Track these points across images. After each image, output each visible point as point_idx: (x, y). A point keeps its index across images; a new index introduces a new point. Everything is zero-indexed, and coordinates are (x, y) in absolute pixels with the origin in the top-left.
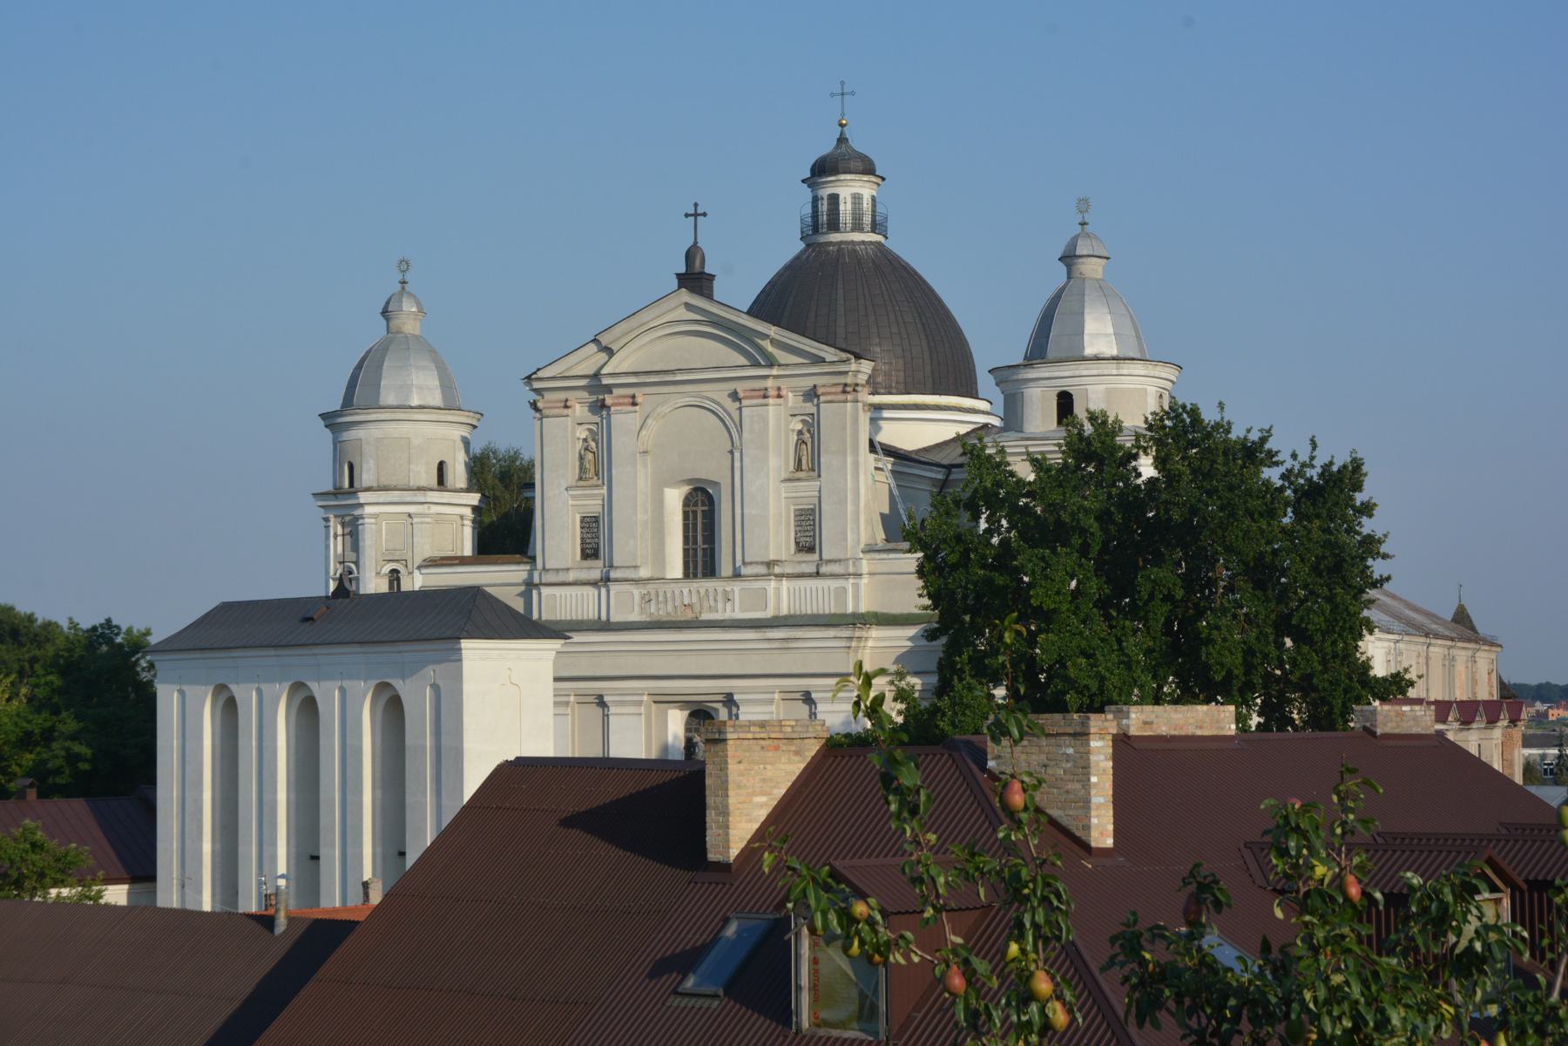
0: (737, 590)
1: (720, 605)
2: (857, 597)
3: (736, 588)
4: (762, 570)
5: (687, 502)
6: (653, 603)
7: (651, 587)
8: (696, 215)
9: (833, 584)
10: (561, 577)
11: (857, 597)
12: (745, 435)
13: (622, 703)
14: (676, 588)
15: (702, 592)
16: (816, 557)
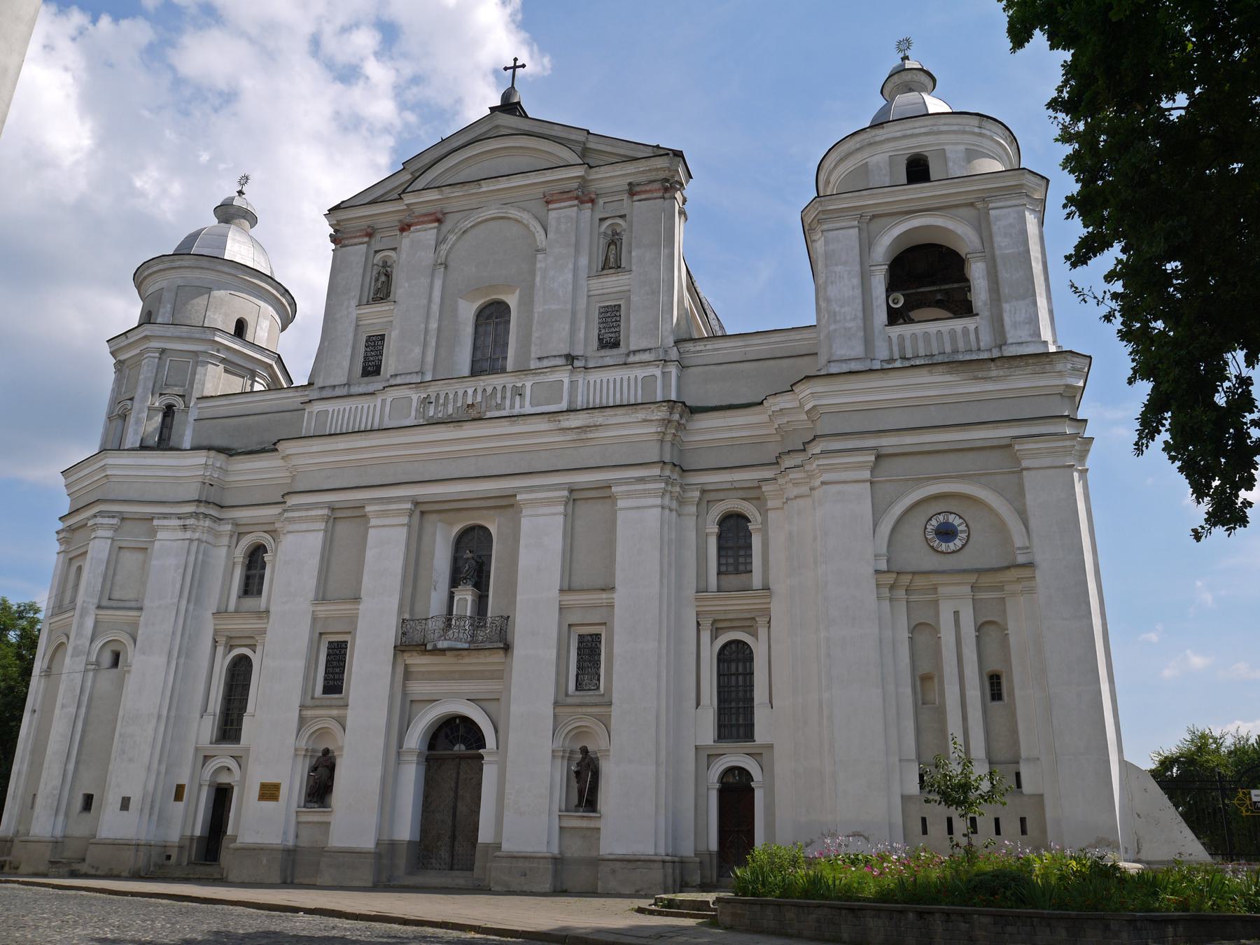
0: (528, 385)
1: (508, 402)
2: (666, 386)
4: (561, 361)
6: (432, 408)
7: (432, 390)
8: (515, 67)
9: (641, 373)
10: (338, 392)
11: (666, 386)
12: (551, 235)
13: (384, 514)
14: (460, 388)
15: (489, 390)
16: (623, 349)
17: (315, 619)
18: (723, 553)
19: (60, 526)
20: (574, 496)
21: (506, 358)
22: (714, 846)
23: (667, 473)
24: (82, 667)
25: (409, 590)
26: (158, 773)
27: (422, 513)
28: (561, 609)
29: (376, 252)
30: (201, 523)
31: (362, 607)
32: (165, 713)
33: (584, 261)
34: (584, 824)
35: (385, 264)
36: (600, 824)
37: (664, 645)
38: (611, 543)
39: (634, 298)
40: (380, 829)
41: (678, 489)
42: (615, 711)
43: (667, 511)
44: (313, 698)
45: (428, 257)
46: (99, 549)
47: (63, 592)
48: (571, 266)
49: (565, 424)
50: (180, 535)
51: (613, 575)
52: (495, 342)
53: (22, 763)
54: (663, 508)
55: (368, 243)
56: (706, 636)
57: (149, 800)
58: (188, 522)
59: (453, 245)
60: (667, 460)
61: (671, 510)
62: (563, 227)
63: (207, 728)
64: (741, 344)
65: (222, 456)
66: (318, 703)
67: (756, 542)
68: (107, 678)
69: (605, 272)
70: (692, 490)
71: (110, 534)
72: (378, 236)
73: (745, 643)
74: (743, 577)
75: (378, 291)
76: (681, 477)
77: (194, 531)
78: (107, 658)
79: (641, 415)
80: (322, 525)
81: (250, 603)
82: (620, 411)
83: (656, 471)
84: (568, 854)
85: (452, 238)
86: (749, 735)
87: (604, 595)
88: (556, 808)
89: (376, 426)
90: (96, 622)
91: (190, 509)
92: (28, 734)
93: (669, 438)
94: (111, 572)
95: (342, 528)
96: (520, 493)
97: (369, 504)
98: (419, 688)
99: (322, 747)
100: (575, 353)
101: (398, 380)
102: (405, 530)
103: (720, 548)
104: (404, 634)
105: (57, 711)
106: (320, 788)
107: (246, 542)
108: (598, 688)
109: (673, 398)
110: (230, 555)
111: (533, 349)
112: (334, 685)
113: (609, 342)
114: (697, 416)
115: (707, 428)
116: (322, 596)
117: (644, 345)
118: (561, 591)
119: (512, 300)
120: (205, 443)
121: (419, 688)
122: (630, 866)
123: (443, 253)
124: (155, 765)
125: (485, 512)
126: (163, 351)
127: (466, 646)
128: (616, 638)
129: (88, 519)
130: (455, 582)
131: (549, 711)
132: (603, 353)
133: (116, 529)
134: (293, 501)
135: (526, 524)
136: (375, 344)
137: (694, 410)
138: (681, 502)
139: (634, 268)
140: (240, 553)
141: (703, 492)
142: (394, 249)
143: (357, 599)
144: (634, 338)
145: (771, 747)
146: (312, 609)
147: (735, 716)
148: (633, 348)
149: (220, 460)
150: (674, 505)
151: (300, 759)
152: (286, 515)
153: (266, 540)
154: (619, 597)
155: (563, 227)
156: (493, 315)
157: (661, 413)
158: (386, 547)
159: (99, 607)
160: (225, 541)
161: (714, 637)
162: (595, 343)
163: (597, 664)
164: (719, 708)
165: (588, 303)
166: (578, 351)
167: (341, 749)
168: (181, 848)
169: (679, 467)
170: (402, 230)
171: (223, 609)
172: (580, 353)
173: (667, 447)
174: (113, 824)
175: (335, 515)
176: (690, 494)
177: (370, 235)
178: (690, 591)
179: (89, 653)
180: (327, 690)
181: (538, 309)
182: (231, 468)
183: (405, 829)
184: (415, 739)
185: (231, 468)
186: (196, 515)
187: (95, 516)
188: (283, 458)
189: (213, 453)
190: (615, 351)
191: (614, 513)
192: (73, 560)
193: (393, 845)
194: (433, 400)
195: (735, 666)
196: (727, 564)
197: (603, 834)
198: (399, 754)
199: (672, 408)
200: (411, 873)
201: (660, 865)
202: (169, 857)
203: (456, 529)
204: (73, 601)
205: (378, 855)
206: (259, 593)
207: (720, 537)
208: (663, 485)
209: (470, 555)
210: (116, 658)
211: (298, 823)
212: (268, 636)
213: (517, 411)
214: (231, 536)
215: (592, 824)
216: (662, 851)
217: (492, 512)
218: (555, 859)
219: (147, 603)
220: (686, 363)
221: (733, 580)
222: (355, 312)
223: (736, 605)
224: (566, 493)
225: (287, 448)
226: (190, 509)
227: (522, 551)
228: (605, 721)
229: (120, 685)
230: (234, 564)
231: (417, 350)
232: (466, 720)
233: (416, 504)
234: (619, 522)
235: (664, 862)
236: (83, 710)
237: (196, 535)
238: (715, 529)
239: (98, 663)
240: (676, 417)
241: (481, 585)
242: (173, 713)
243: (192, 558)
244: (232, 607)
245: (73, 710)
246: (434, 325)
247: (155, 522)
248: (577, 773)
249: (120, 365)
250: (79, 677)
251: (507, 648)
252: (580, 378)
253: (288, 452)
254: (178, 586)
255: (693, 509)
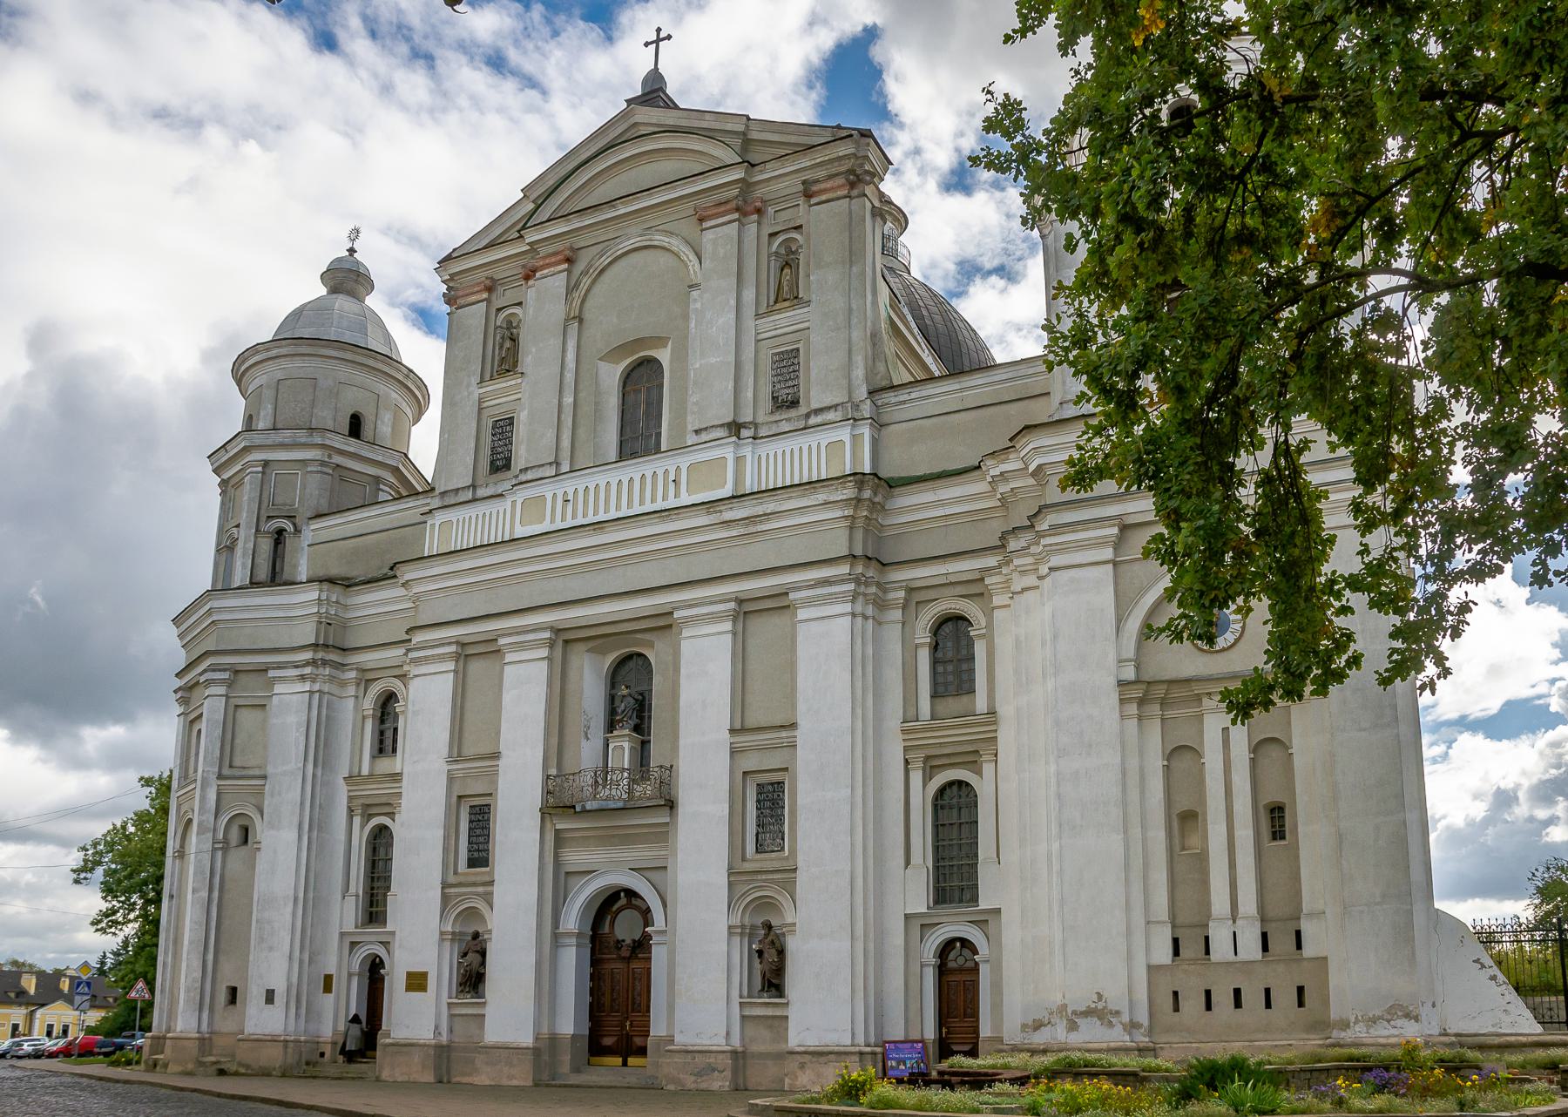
3: (684, 461)
5: (628, 378)
9: (825, 437)
12: (707, 264)
13: (521, 646)
16: (803, 410)
17: (451, 779)
18: (940, 669)
19: (179, 683)
20: (745, 611)
21: (659, 435)
22: (930, 1033)
23: (859, 569)
24: (209, 846)
25: (554, 741)
26: (301, 962)
27: (566, 642)
28: (734, 752)
29: (499, 310)
30: (321, 670)
31: (502, 763)
32: (301, 895)
33: (749, 294)
34: (769, 1012)
35: (509, 325)
36: (793, 1013)
37: (859, 792)
38: (791, 666)
39: (814, 338)
40: (537, 1023)
41: (873, 589)
42: (802, 878)
43: (859, 620)
44: (456, 873)
45: (558, 310)
46: (212, 706)
47: (187, 760)
48: (733, 302)
49: (728, 516)
50: (299, 687)
51: (794, 707)
52: (647, 413)
53: (166, 953)
54: (854, 615)
55: (488, 300)
56: (916, 778)
57: (294, 992)
58: (308, 670)
59: (588, 291)
60: (859, 551)
61: (865, 617)
62: (722, 251)
63: (345, 913)
64: (957, 386)
65: (338, 589)
66: (461, 879)
67: (980, 649)
68: (237, 856)
69: (778, 306)
70: (895, 589)
71: (222, 690)
72: (500, 289)
73: (968, 784)
74: (965, 699)
75: (502, 360)
76: (881, 572)
77: (314, 681)
78: (235, 835)
79: (821, 497)
80: (451, 666)
81: (385, 765)
82: (795, 492)
83: (844, 569)
84: (755, 1048)
85: (586, 281)
86: (974, 899)
87: (784, 734)
88: (735, 993)
89: (507, 538)
90: (219, 794)
91: (308, 655)
92: (169, 922)
93: (860, 523)
94: (229, 736)
95: (475, 667)
96: (677, 609)
97: (503, 635)
98: (576, 858)
99: (471, 930)
100: (741, 421)
101: (529, 475)
102: (545, 664)
103: (935, 662)
104: (548, 792)
105: (189, 896)
106: (472, 980)
107: (376, 689)
108: (783, 849)
109: (867, 471)
110: (356, 707)
111: (689, 419)
112: (479, 858)
113: (786, 403)
114: (897, 491)
115: (914, 506)
116: (457, 753)
117: (827, 402)
118: (732, 731)
119: (664, 356)
120: (321, 573)
121: (576, 858)
122: (822, 1059)
123: (577, 303)
124: (297, 953)
125: (639, 636)
126: (266, 464)
127: (620, 805)
128: (800, 786)
129: (201, 674)
130: (611, 726)
131: (723, 880)
132: (777, 417)
133: (230, 684)
134: (418, 638)
135: (685, 646)
136: (504, 428)
137: (893, 484)
138: (881, 605)
139: (814, 297)
140: (369, 704)
141: (910, 590)
142: (520, 304)
143: (496, 756)
144: (816, 397)
145: (998, 911)
146: (446, 767)
147: (954, 876)
148: (815, 405)
149: (335, 594)
150: (870, 610)
151: (447, 944)
152: (411, 655)
153: (397, 686)
154: (801, 735)
155: (722, 251)
156: (642, 379)
157: (849, 492)
158: (523, 688)
159: (220, 777)
160: (351, 690)
161: (927, 778)
162: (766, 403)
163: (780, 819)
164: (937, 868)
165: (756, 352)
166: (747, 416)
167: (490, 932)
168: (334, 1043)
169: (873, 562)
170: (527, 278)
171: (356, 772)
172: (749, 419)
173: (859, 535)
174: (263, 1021)
175: (465, 653)
176: (892, 595)
177: (490, 289)
178: (893, 721)
179: (215, 830)
180: (472, 863)
181: (696, 363)
182: (350, 601)
183: (569, 1021)
184: (572, 919)
185: (350, 601)
186: (313, 663)
187: (205, 671)
188: (403, 585)
189: (325, 586)
190: (793, 413)
191: (794, 626)
192: (191, 722)
193: (554, 1039)
194: (570, 497)
195: (955, 813)
196: (946, 684)
197: (791, 1024)
198: (556, 937)
199: (862, 482)
200: (577, 1070)
201: (856, 1058)
202: (322, 1055)
203: (610, 659)
204: (196, 771)
205: (536, 1051)
206: (394, 750)
207: (935, 647)
208: (852, 586)
209: (625, 692)
210: (245, 832)
211: (452, 1016)
212: (404, 801)
213: (672, 502)
214: (358, 685)
215: (778, 1012)
216: (861, 1040)
217: (647, 636)
218: (734, 1053)
219: (270, 770)
220: (885, 419)
221: (952, 705)
222: (477, 392)
223: (955, 736)
224: (732, 605)
225: (408, 573)
226: (308, 655)
227: (683, 681)
228: (789, 887)
229: (251, 865)
230: (364, 718)
231: (551, 434)
232: (631, 894)
233: (557, 631)
234: (799, 639)
235: (861, 1053)
236: (216, 894)
237: (316, 687)
238: (923, 637)
239: (226, 841)
240: (867, 494)
241: (641, 727)
242: (311, 895)
243: (315, 712)
244: (365, 771)
245: (206, 895)
246: (569, 400)
247: (271, 673)
248: (760, 953)
249: (224, 484)
250: (207, 857)
251: (671, 805)
252: (747, 451)
253: (408, 577)
254: (302, 748)
255: (897, 614)
